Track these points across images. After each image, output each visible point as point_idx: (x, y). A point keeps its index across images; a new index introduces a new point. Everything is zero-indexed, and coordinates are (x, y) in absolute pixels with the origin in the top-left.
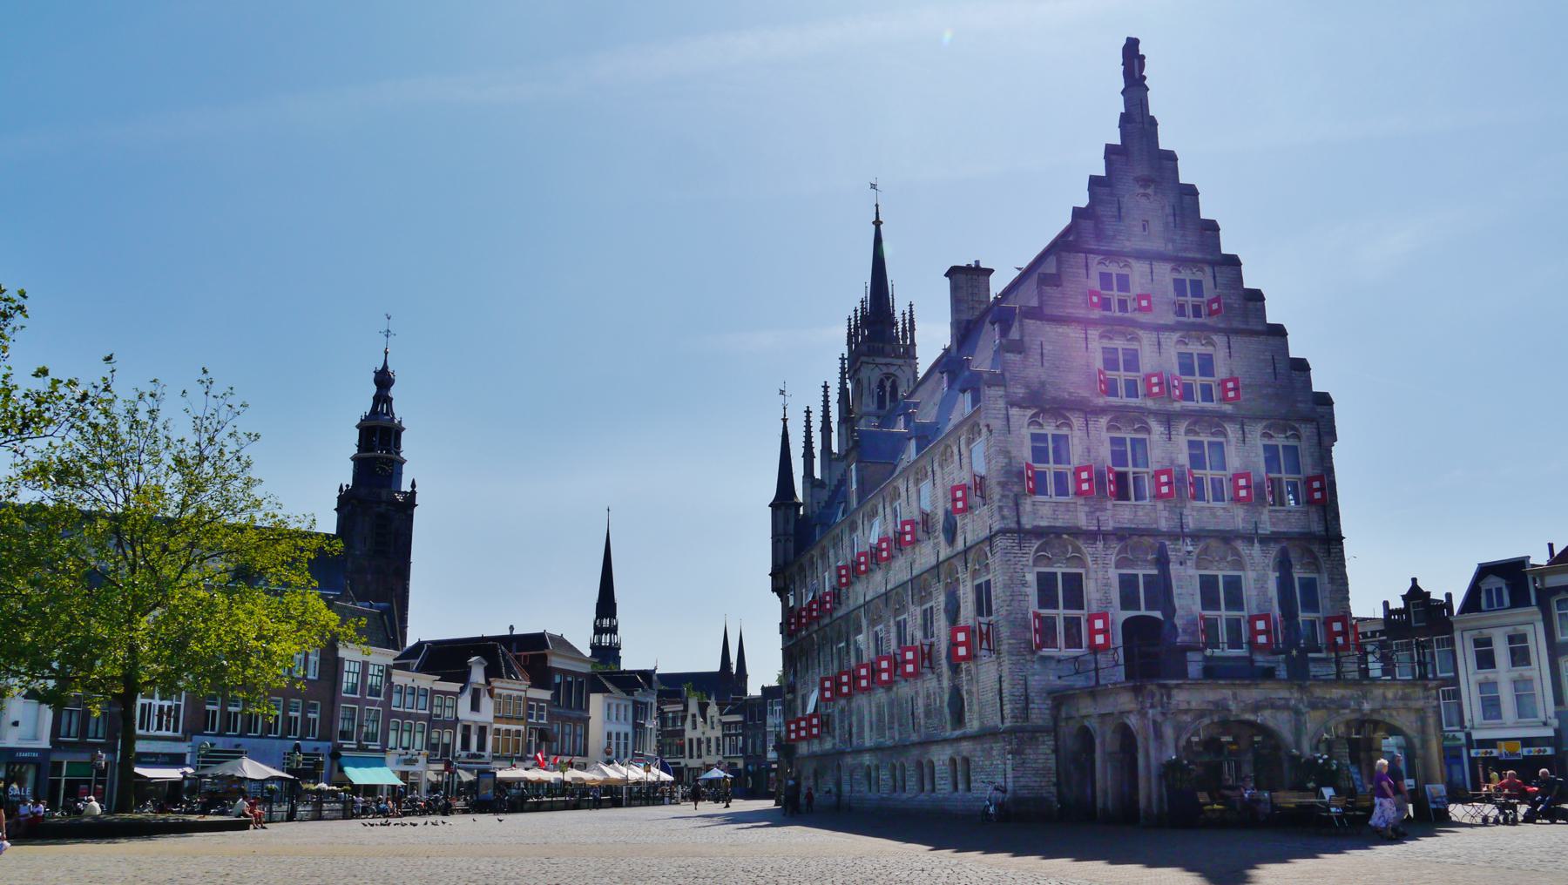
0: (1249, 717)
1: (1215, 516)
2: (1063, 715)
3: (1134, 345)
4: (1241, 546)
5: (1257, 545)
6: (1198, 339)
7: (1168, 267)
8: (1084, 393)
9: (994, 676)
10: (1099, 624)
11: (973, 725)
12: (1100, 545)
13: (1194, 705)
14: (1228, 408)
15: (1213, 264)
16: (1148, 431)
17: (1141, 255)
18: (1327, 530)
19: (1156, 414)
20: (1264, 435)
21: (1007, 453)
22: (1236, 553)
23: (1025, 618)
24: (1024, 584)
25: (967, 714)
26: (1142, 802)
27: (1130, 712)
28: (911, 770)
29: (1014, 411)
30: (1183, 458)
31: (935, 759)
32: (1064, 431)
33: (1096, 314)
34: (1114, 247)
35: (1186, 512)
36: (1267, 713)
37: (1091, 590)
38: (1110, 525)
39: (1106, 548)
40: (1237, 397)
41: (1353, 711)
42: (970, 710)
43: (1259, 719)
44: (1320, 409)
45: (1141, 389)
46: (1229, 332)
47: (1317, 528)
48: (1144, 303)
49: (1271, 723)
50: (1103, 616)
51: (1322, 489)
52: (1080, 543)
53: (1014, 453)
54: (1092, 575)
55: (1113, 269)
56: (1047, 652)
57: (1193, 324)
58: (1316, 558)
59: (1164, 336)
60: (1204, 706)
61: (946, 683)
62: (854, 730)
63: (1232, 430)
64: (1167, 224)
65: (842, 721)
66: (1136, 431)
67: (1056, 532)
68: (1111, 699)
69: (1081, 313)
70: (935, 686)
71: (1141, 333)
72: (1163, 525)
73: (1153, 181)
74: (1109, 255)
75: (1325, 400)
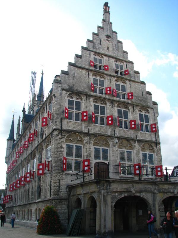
0: (138, 194)
1: (125, 133)
2: (72, 194)
3: (103, 79)
4: (132, 143)
5: (137, 143)
6: (122, 81)
7: (113, 60)
8: (86, 90)
9: (49, 180)
10: (86, 163)
11: (42, 198)
12: (89, 137)
13: (119, 189)
14: (129, 101)
16: (106, 104)
17: (106, 55)
18: (156, 140)
19: (108, 99)
20: (139, 111)
21: (60, 105)
22: (131, 144)
23: (61, 160)
24: (63, 148)
25: (41, 194)
26: (97, 228)
27: (94, 192)
28: (26, 212)
29: (63, 92)
30: (116, 114)
31: (32, 209)
32: (79, 100)
33: (92, 68)
34: (98, 51)
35: (116, 130)
36: (144, 194)
37: (85, 153)
38: (92, 131)
39: (90, 139)
40: (132, 98)
41: (171, 193)
42: (42, 192)
43: (141, 195)
44: (155, 106)
45: (104, 92)
46: (130, 81)
47: (154, 139)
48: (106, 68)
49: (145, 197)
50: (88, 161)
51: (155, 128)
52: (82, 136)
53: (62, 105)
54: (85, 147)
56: (67, 172)
57: (120, 76)
58: (153, 148)
59: (112, 78)
60: (122, 190)
61: (37, 184)
62: (16, 200)
63: (131, 108)
64: (113, 49)
65: (14, 197)
66: (102, 103)
67: (75, 132)
68: (88, 187)
69: (87, 67)
70: (33, 185)
71: (105, 76)
72: (109, 134)
75: (155, 104)
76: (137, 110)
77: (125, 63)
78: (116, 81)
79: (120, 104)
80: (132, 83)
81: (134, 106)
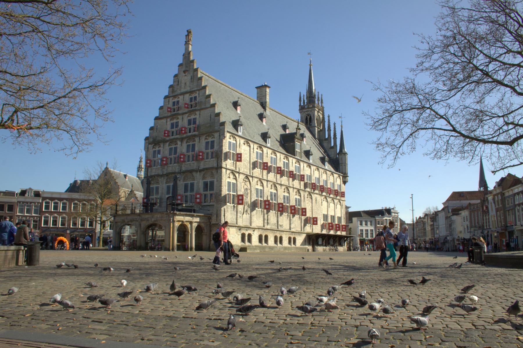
1: (190, 165)
4: (194, 174)
7: (188, 95)
12: (163, 178)
15: (199, 90)
16: (176, 144)
20: (206, 139)
29: (150, 146)
30: (184, 150)
34: (176, 94)
38: (165, 173)
46: (200, 110)
47: (215, 165)
55: (176, 100)
63: (197, 139)
69: (166, 115)
72: (177, 171)
73: (187, 71)
74: (175, 97)
76: (203, 139)
77: (198, 92)
78: (188, 116)
79: (189, 138)
80: (202, 112)
81: (199, 136)
